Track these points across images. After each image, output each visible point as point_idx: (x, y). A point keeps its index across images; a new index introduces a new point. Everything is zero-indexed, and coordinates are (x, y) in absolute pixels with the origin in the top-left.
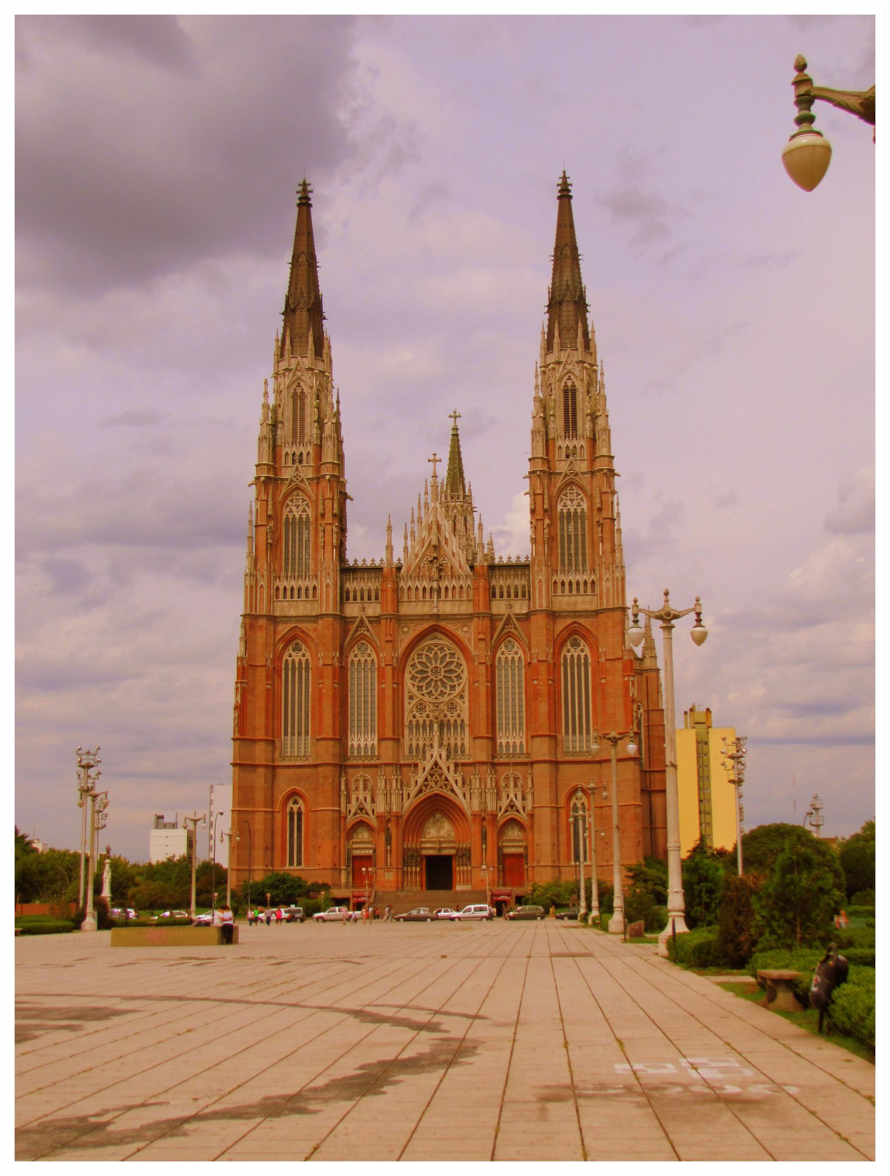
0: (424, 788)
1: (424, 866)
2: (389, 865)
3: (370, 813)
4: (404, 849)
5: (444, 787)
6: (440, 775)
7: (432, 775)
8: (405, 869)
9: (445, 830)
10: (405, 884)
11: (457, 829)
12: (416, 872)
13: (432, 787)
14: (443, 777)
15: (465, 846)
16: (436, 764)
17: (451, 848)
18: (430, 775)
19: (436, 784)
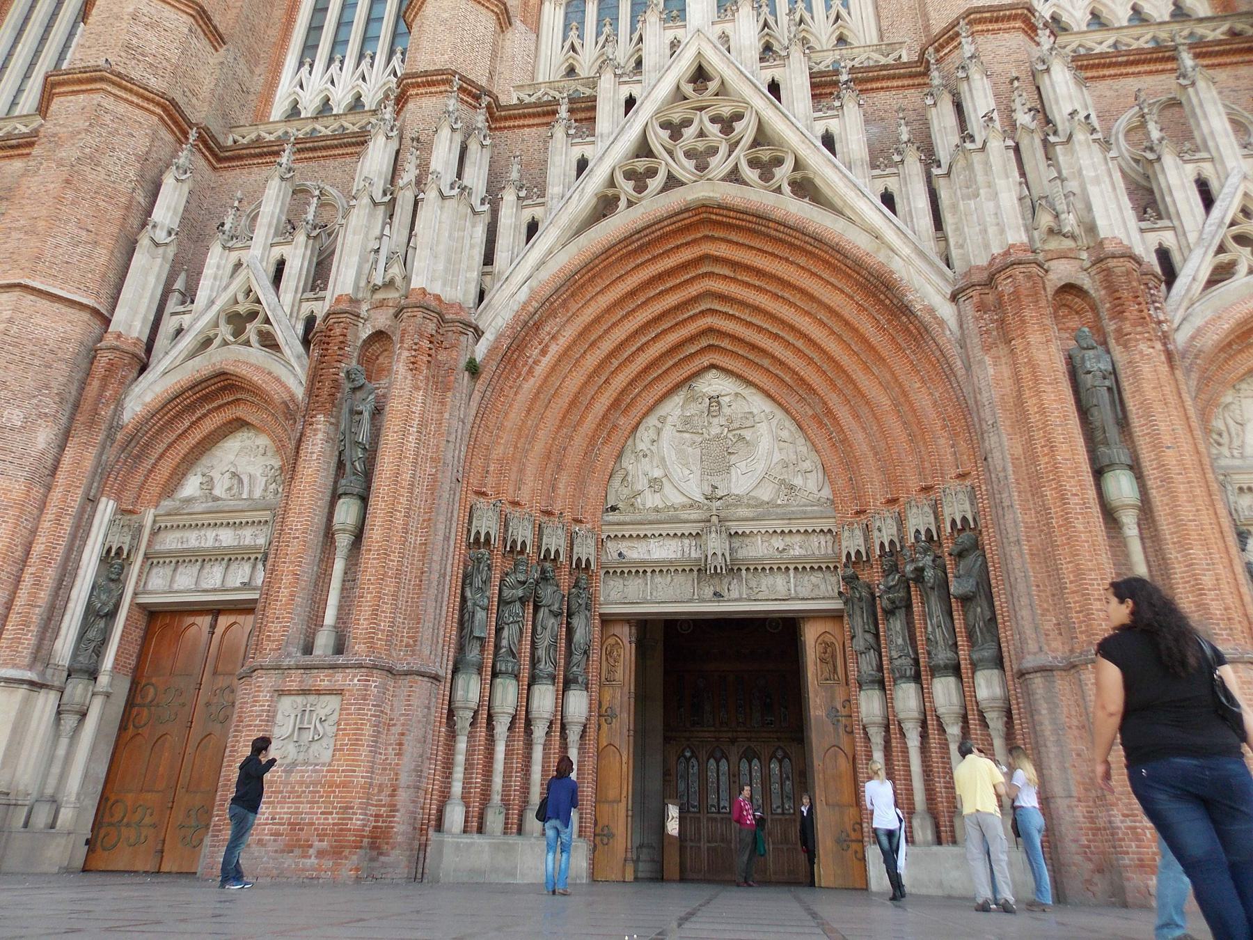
0: (627, 187)
1: (621, 696)
2: (324, 641)
3: (289, 335)
4: (479, 542)
5: (751, 174)
6: (727, 124)
7: (675, 130)
8: (470, 689)
9: (761, 467)
10: (455, 815)
11: (841, 443)
12: (560, 724)
13: (672, 182)
14: (745, 130)
15: (919, 520)
16: (700, 75)
17: (802, 568)
18: (666, 125)
19: (702, 167)
